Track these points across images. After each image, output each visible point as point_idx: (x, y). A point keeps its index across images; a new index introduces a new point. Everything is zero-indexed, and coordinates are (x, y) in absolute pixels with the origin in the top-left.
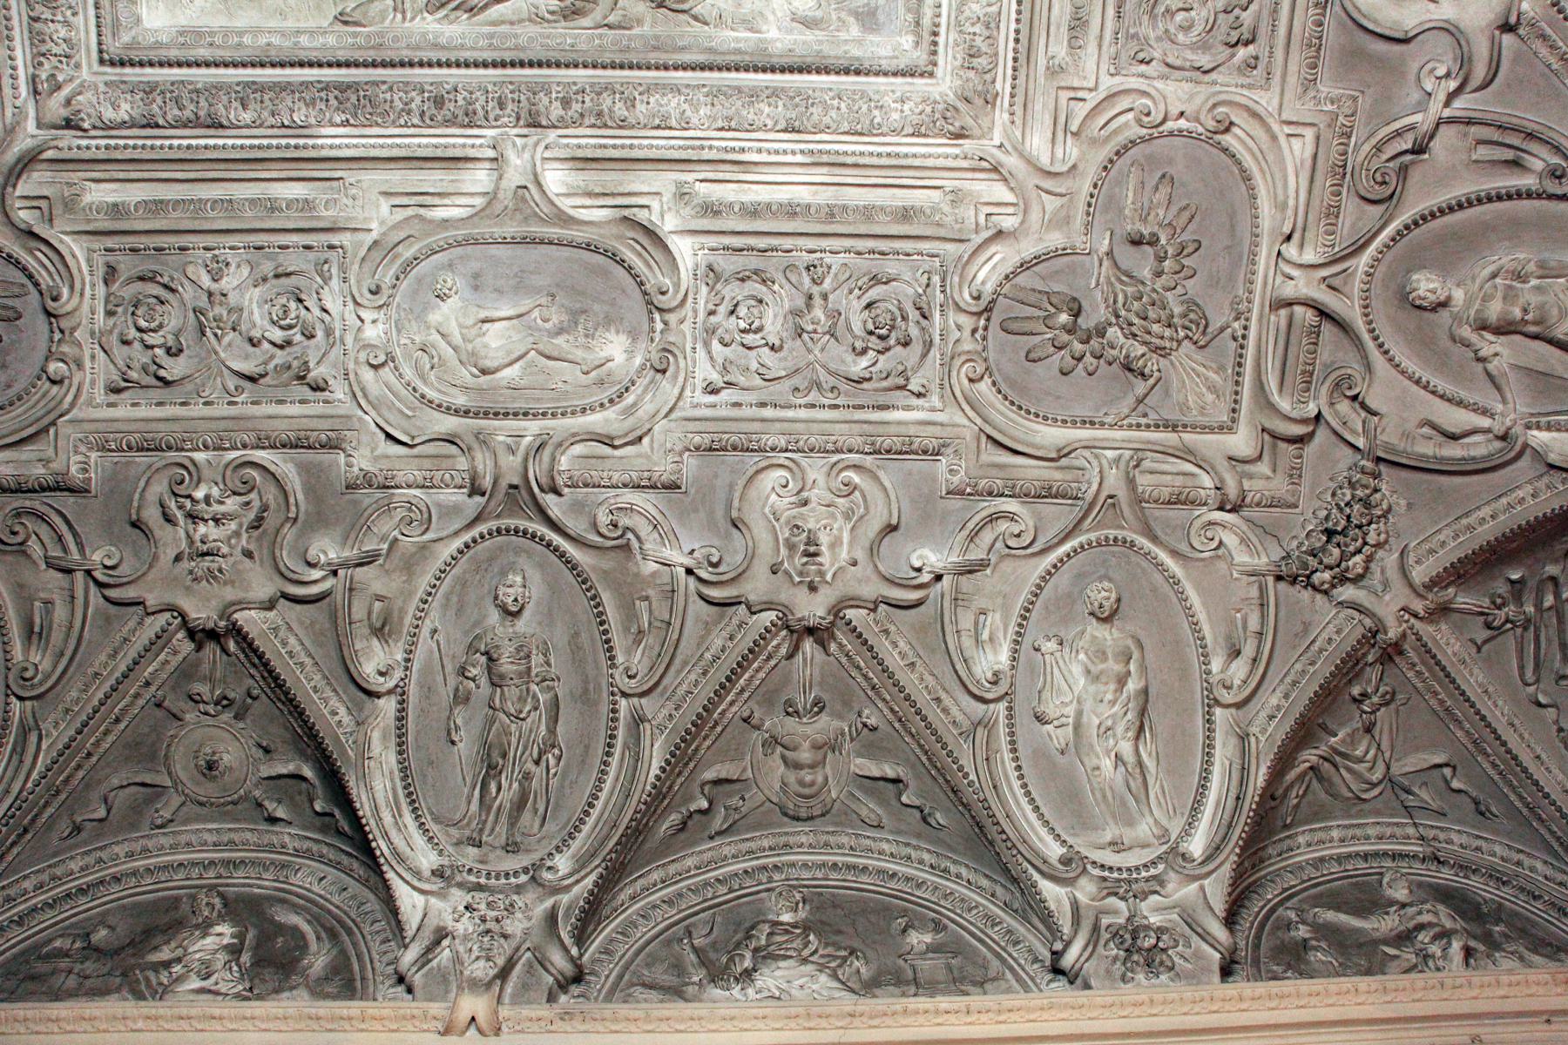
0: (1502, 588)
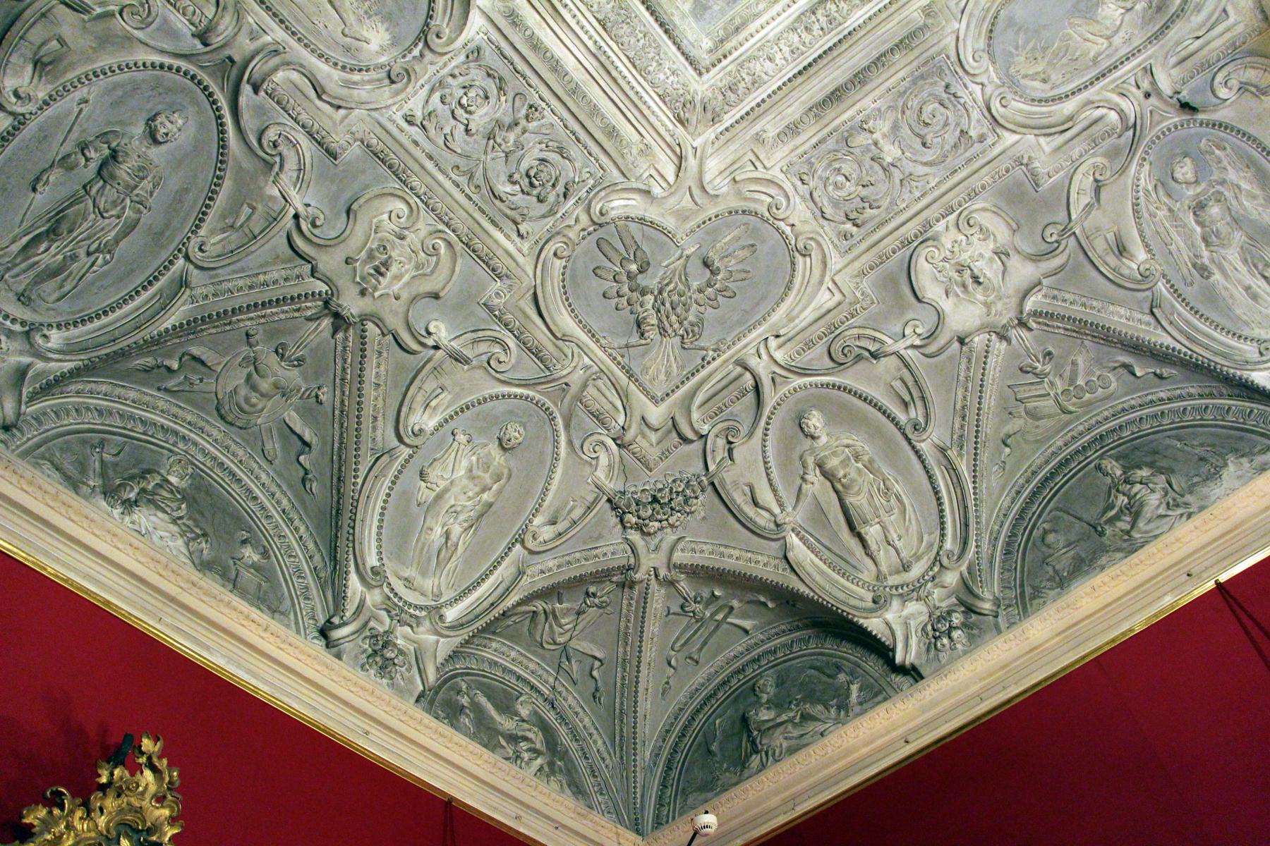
0: (706, 594)
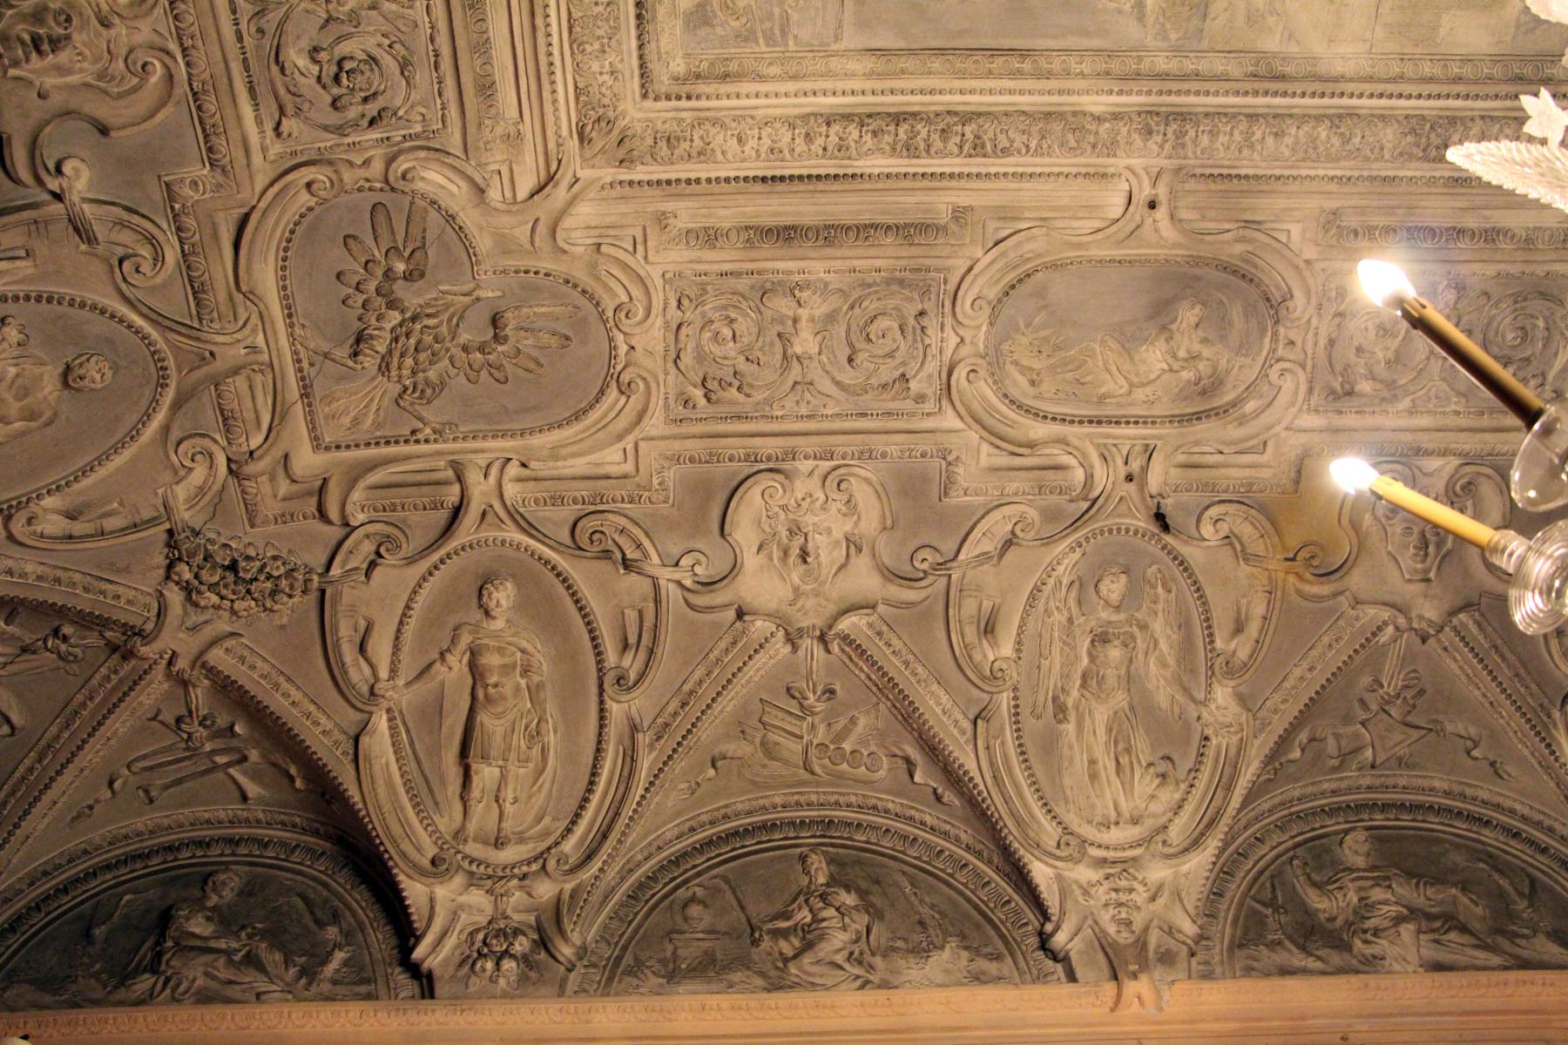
0: (222, 721)
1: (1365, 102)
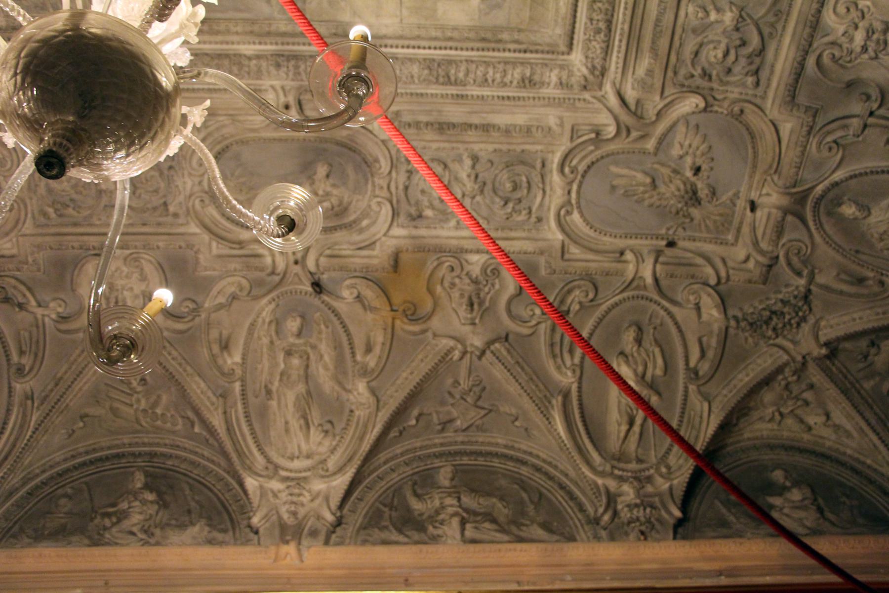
1: (400, 50)
